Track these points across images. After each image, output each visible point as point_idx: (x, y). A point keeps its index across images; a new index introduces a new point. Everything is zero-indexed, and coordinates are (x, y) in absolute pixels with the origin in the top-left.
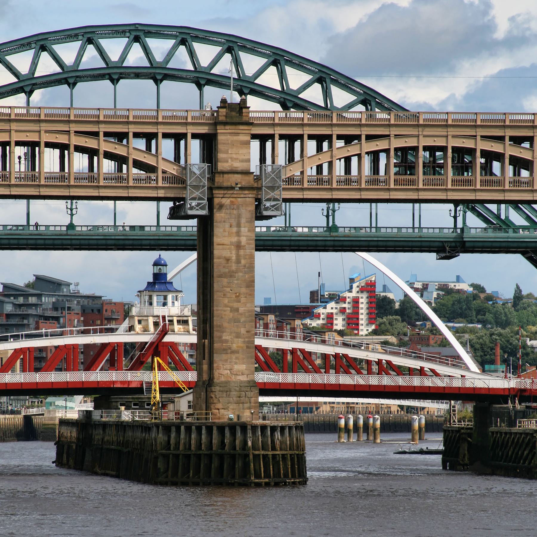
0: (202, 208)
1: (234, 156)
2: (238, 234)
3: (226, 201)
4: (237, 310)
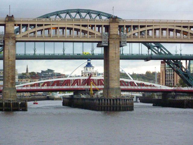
0: (106, 44)
1: (114, 31)
2: (115, 50)
3: (112, 42)
4: (115, 69)
